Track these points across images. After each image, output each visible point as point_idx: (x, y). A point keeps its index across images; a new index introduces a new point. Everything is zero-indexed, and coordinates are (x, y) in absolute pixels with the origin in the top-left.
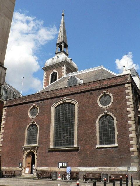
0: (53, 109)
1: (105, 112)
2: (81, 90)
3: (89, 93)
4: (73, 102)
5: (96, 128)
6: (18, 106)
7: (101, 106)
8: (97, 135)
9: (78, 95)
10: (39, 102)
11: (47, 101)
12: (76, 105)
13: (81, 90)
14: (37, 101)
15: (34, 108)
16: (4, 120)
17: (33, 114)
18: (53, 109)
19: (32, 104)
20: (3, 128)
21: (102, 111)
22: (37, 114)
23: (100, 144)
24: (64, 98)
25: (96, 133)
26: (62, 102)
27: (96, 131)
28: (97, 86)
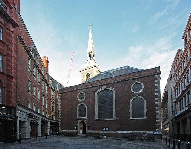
0: (96, 94)
1: (137, 96)
2: (117, 80)
3: (123, 83)
4: (112, 89)
5: (129, 107)
6: (69, 93)
7: (133, 92)
8: (131, 111)
9: (115, 84)
10: (85, 90)
11: (90, 89)
12: (114, 91)
13: (117, 80)
14: (83, 89)
15: (81, 93)
16: (60, 102)
17: (80, 98)
18: (96, 94)
19: (79, 91)
20: (60, 108)
21: (135, 95)
22: (84, 98)
23: (132, 117)
24: (105, 87)
25: (130, 110)
26: (102, 89)
27: (130, 108)
28: (130, 77)
